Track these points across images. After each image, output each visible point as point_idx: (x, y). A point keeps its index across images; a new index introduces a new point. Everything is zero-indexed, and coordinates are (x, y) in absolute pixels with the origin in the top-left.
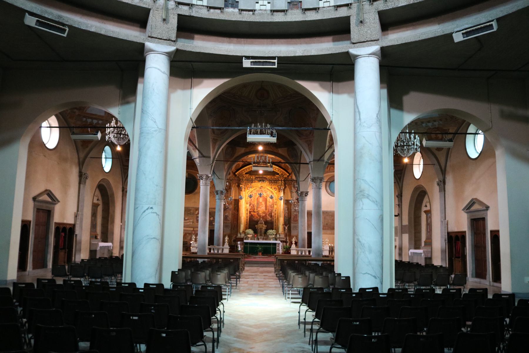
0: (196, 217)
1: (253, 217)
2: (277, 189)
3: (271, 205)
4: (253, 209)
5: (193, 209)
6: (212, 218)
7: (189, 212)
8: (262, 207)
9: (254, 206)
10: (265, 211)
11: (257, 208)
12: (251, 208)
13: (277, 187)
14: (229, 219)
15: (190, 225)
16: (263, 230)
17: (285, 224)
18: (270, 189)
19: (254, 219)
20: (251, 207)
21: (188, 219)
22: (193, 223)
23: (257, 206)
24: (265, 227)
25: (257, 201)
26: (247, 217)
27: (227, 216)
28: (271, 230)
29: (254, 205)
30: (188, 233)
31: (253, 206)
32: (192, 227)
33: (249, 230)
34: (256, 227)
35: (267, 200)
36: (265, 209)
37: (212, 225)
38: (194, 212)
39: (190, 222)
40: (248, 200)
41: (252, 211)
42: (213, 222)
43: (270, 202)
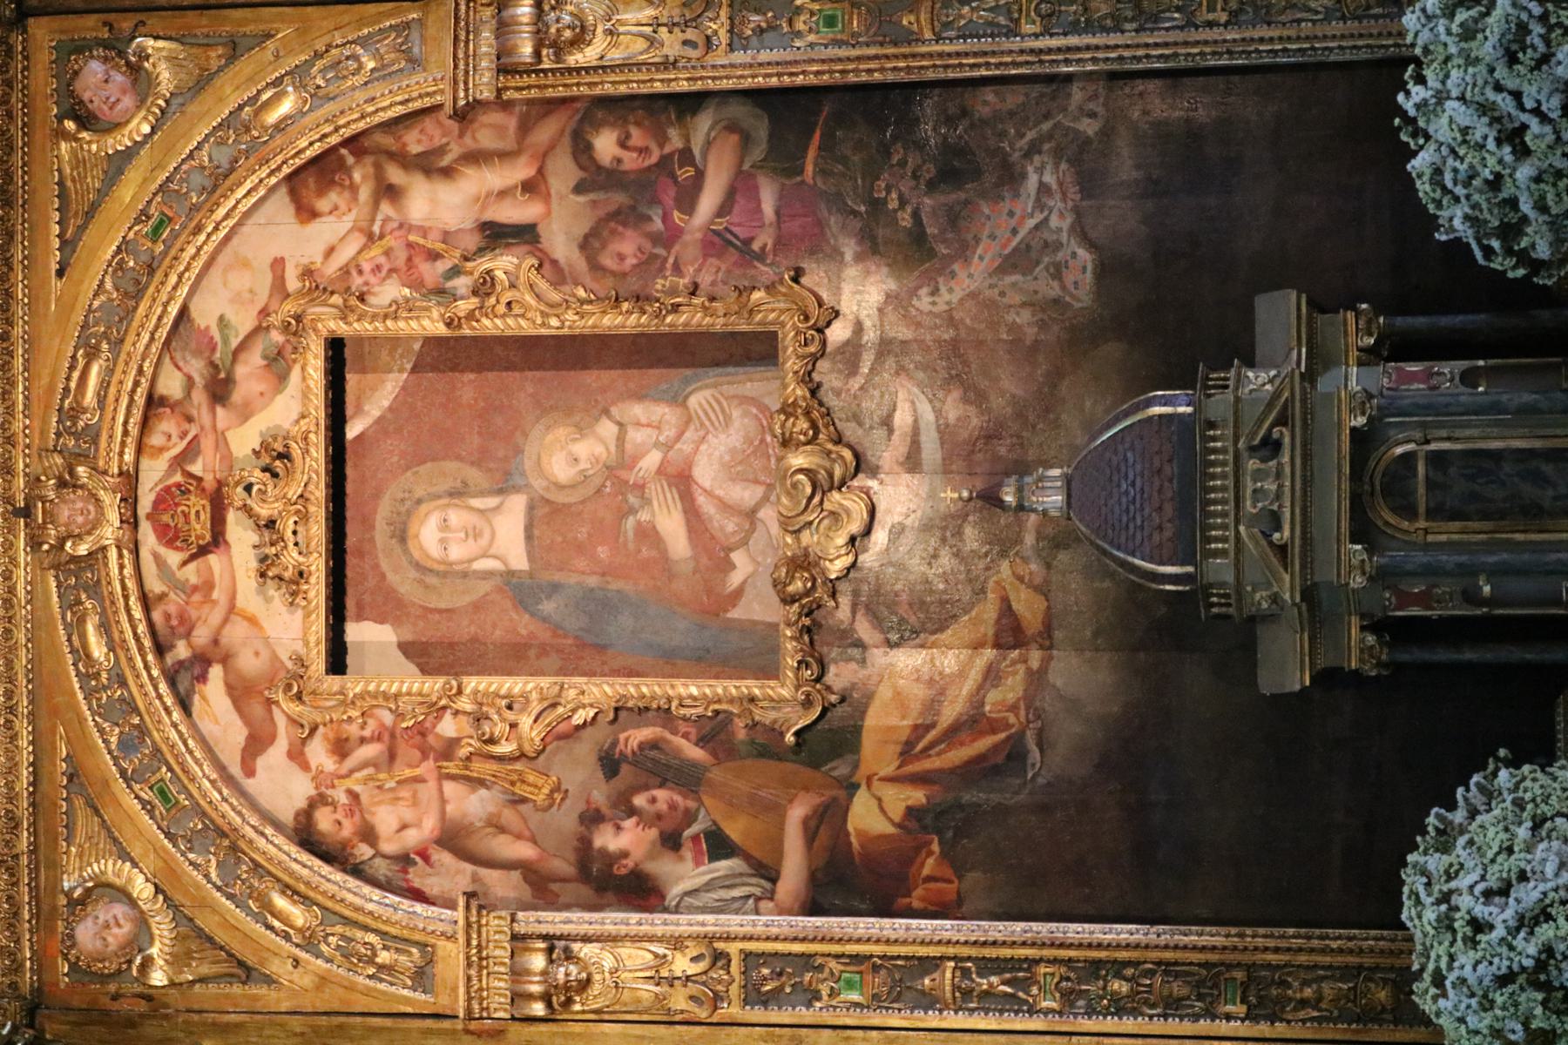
1: (1014, 754)
2: (90, 26)
3: (595, 178)
4: (761, 777)
8: (681, 481)
9: (636, 736)
10: (792, 363)
11: (706, 662)
12: (718, 845)
13: (43, 33)
16: (1433, 412)
18: (102, 246)
19: (1068, 731)
20: (671, 842)
23: (672, 662)
24: (1320, 360)
25: (514, 657)
26: (1019, 970)
28: (1412, 98)
29: (610, 764)
31: (662, 795)
33: (1420, 917)
34: (1328, 678)
35: (432, 324)
36: (757, 385)
40: (452, 957)
41: (797, 813)
43: (496, 235)
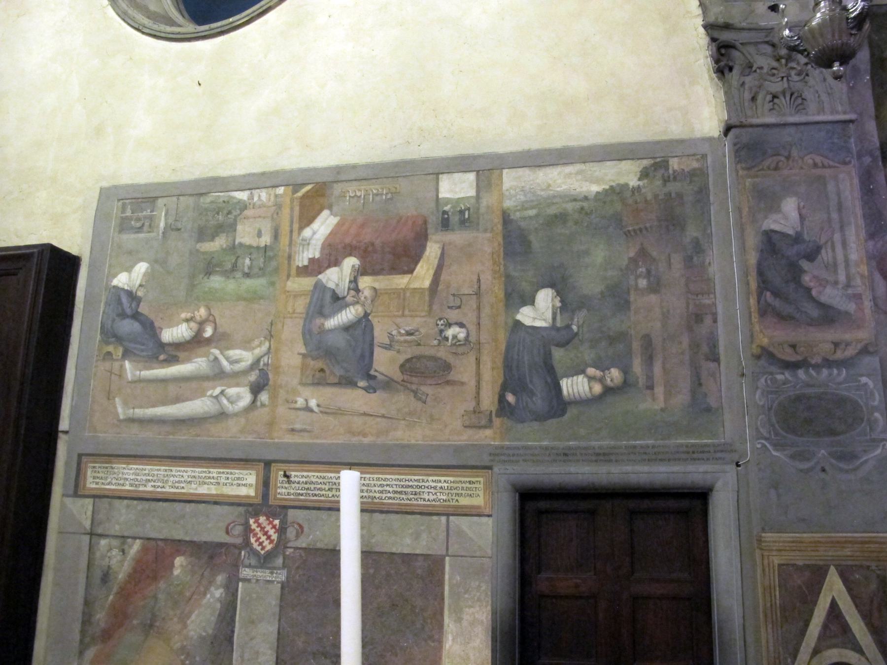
0: (301, 305)
5: (263, 195)
6: (545, 298)
7: (220, 243)
14: (831, 296)
15: (222, 415)
17: (861, 463)
21: (197, 342)
22: (256, 389)
27: (797, 239)
30: (178, 546)
32: (245, 462)
37: (540, 418)
38: (276, 236)
39: (219, 375)
42: (558, 354)
